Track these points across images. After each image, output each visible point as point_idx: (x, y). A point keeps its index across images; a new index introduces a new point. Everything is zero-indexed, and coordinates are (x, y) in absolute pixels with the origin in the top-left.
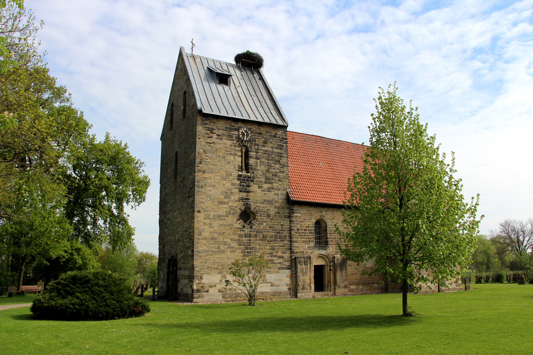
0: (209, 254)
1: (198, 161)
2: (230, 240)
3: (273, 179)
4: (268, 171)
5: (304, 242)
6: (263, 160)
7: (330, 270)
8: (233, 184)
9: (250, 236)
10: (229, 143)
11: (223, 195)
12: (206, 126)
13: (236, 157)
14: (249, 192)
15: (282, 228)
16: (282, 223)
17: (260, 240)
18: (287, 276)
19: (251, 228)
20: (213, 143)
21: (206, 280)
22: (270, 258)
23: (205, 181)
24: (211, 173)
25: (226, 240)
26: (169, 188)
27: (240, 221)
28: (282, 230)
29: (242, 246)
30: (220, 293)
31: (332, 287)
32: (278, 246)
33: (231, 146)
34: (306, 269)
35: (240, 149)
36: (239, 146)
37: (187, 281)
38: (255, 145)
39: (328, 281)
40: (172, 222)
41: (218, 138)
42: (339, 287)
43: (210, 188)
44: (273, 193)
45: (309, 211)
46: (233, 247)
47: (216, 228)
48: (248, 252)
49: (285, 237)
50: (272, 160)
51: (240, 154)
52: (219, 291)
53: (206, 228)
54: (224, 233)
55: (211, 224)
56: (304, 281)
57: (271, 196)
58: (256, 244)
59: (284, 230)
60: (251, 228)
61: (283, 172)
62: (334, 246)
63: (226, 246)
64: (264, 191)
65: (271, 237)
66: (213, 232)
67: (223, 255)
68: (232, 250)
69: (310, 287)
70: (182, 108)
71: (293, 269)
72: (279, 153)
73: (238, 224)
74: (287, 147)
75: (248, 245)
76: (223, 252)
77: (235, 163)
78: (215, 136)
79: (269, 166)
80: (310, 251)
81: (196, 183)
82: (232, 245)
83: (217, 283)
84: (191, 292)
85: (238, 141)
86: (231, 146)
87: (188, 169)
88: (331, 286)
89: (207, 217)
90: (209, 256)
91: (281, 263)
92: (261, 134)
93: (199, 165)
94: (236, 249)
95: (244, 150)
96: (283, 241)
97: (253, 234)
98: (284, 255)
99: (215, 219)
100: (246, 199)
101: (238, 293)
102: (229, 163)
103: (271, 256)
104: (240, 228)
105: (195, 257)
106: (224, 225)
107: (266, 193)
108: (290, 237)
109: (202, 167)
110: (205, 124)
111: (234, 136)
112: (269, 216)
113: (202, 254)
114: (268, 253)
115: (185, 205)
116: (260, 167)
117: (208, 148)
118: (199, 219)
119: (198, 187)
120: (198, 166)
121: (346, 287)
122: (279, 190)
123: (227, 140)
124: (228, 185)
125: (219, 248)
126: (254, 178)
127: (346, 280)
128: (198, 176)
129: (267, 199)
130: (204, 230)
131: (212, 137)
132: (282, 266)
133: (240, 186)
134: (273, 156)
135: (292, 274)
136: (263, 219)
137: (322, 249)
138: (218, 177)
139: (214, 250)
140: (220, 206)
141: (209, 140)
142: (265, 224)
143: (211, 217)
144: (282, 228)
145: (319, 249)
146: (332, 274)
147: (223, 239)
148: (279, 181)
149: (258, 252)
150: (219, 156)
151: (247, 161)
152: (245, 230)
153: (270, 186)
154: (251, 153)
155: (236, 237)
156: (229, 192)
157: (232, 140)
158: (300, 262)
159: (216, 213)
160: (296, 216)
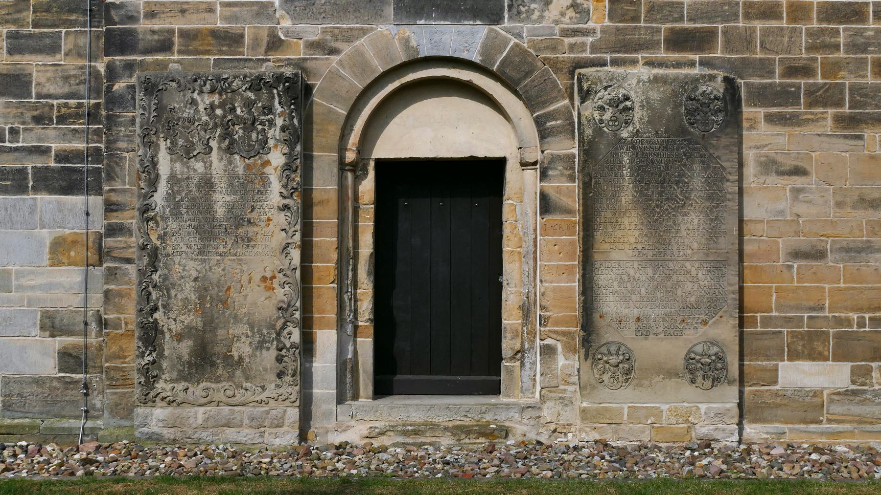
34: (249, 188)
56: (213, 300)
71: (125, 186)
80: (313, 31)
98: (35, 65)
135: (113, 230)
158: (164, 123)
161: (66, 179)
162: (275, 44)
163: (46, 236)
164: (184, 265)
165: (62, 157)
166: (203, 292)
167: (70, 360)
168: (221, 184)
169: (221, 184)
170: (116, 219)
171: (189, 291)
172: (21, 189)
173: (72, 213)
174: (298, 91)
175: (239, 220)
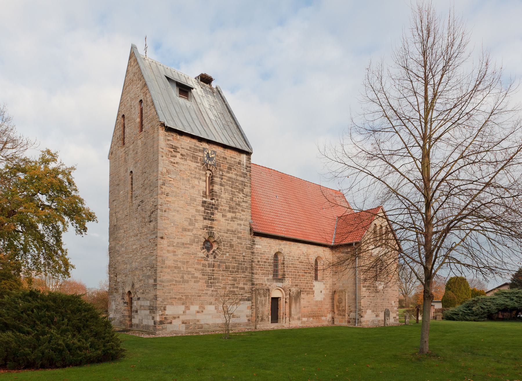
2: (193, 270)
4: (232, 199)
5: (263, 274)
6: (227, 187)
7: (286, 302)
8: (197, 211)
13: (200, 182)
14: (213, 220)
15: (244, 259)
16: (244, 255)
17: (223, 270)
18: (248, 307)
19: (215, 257)
21: (170, 311)
22: (232, 289)
23: (169, 205)
25: (189, 269)
28: (244, 262)
29: (205, 277)
30: (184, 325)
31: (288, 319)
32: (240, 277)
34: (265, 301)
36: (204, 170)
37: (148, 312)
39: (283, 313)
42: (293, 319)
43: (174, 213)
45: (269, 243)
46: (196, 277)
47: (180, 256)
48: (211, 283)
49: (246, 268)
51: (205, 178)
52: (183, 323)
53: (170, 255)
54: (188, 262)
55: (175, 252)
56: (263, 313)
57: (234, 226)
58: (219, 274)
60: (215, 257)
62: (290, 279)
63: (190, 276)
69: (269, 318)
71: (254, 300)
72: (242, 181)
73: (202, 254)
74: (250, 176)
75: (211, 275)
76: (187, 282)
77: (200, 188)
79: (233, 194)
80: (269, 283)
83: (181, 315)
84: (153, 324)
88: (286, 318)
89: (171, 244)
90: (172, 286)
94: (200, 279)
95: (208, 175)
96: (244, 272)
97: (217, 264)
98: (245, 286)
99: (178, 247)
100: (210, 227)
101: (201, 325)
102: (193, 187)
103: (233, 288)
106: (187, 253)
107: (229, 222)
108: (252, 268)
112: (231, 246)
115: (145, 230)
118: (162, 246)
121: (299, 319)
122: (242, 220)
124: (193, 211)
125: (183, 277)
126: (218, 205)
127: (300, 312)
130: (167, 257)
133: (205, 213)
134: (237, 184)
135: (252, 305)
136: (226, 249)
137: (280, 282)
138: (182, 202)
139: (177, 279)
140: (185, 233)
142: (227, 254)
143: (174, 244)
144: (244, 259)
145: (277, 282)
146: (287, 306)
147: (187, 268)
148: (243, 211)
152: (209, 259)
153: (233, 215)
154: (215, 179)
155: (200, 267)
156: (193, 219)
158: (259, 294)
159: (180, 241)
160: (257, 248)
163: (247, 306)
164: (260, 309)
167: (249, 320)
171: (261, 312)
173: (249, 303)
174: (269, 290)
175: (265, 304)
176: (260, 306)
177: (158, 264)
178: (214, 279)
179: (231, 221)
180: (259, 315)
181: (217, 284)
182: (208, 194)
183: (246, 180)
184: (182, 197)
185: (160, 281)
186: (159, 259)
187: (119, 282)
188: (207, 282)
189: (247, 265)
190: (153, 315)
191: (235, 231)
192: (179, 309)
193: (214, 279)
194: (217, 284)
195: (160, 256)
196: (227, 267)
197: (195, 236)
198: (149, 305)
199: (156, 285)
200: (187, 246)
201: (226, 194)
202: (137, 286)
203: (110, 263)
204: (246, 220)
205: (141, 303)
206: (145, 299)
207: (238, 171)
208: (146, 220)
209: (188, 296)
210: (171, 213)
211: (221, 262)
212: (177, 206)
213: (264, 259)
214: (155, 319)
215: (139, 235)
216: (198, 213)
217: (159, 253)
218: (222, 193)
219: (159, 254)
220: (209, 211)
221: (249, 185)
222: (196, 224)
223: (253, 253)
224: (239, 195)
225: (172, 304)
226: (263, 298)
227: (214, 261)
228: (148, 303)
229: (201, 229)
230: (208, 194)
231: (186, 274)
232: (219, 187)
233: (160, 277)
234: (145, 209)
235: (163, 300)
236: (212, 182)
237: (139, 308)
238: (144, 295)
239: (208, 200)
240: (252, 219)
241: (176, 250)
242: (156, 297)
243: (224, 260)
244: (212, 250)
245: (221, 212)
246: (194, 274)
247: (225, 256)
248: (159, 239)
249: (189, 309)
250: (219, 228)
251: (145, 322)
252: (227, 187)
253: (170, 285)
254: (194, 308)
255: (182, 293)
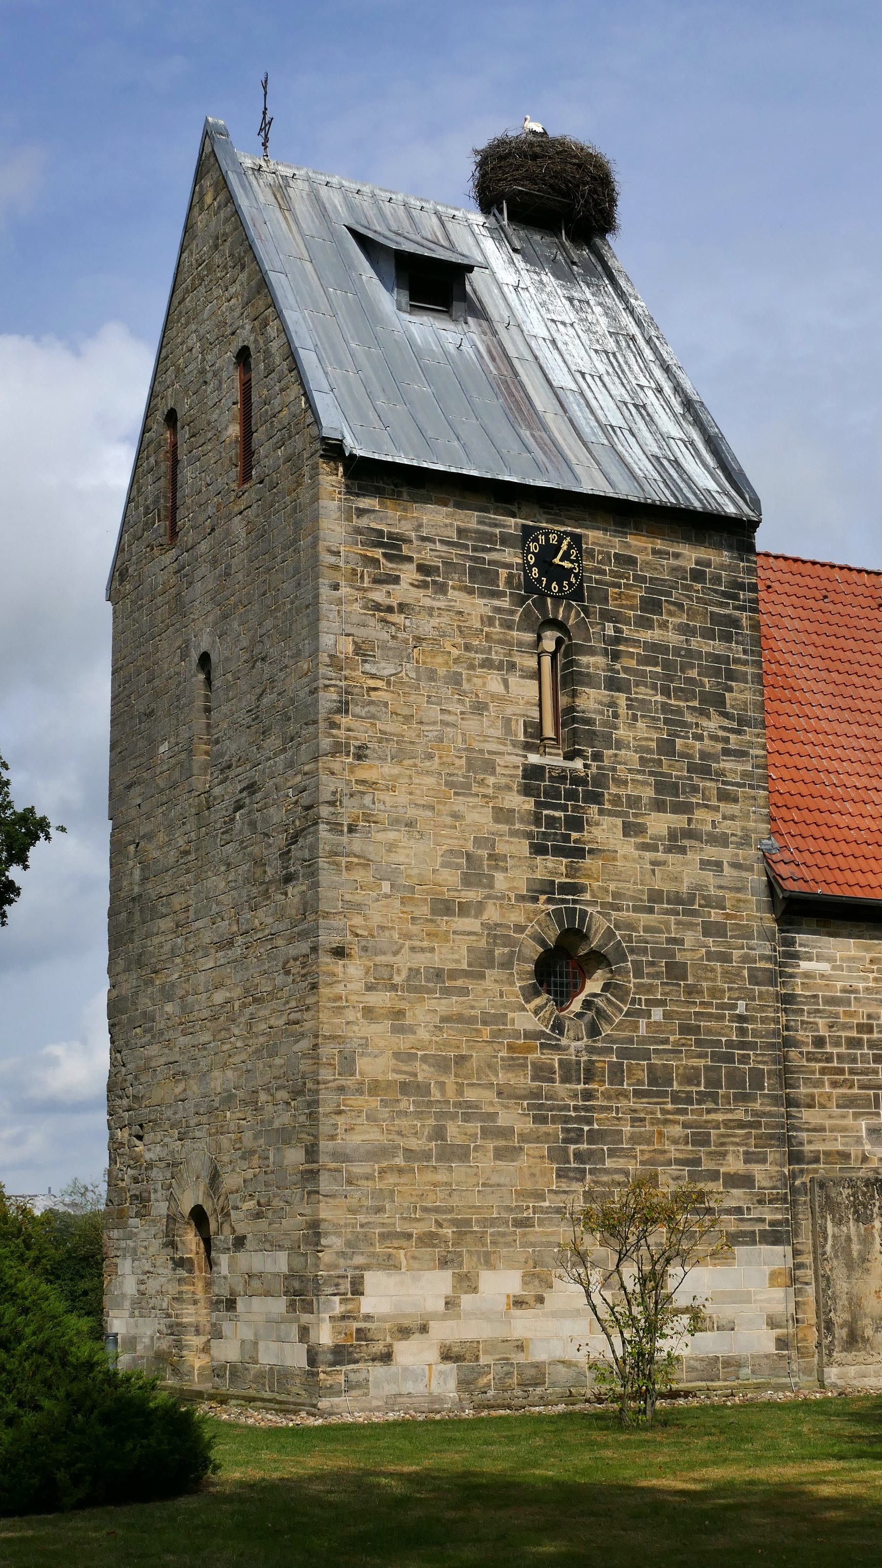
0: (391, 1168)
1: (328, 699)
2: (490, 1095)
3: (695, 789)
4: (667, 747)
5: (848, 1102)
6: (642, 693)
8: (502, 815)
9: (590, 1075)
10: (478, 607)
11: (458, 867)
12: (364, 522)
13: (513, 680)
14: (579, 853)
15: (742, 1032)
16: (741, 1009)
17: (638, 1094)
18: (773, 1276)
19: (594, 1031)
20: (402, 608)
24: (398, 758)
25: (471, 1095)
26: (162, 837)
27: (538, 1001)
28: (743, 1045)
29: (550, 1128)
30: (450, 1366)
32: (727, 1124)
33: (490, 621)
35: (529, 637)
37: (279, 1305)
38: (607, 616)
40: (185, 1009)
41: (424, 585)
43: (392, 835)
44: (693, 857)
45: (868, 949)
46: (506, 1133)
47: (423, 1034)
48: (578, 1156)
49: (757, 1077)
50: (685, 694)
51: (532, 663)
52: (447, 1356)
53: (378, 1032)
54: (461, 1059)
55: (399, 1014)
56: (855, 1303)
57: (686, 871)
58: (619, 1111)
59: (753, 1046)
60: (594, 1031)
61: (741, 754)
63: (475, 1127)
64: (655, 848)
65: (691, 1078)
66: (412, 1057)
67: (459, 1171)
68: (502, 1143)
70: (234, 430)
71: (805, 1240)
72: (717, 658)
73: (527, 1019)
74: (756, 626)
75: (579, 1120)
76: (462, 1154)
77: (509, 710)
78: (408, 573)
79: (674, 722)
81: (325, 811)
82: (503, 1121)
83: (434, 1316)
84: (302, 1362)
85: (522, 600)
86: (490, 621)
87: (273, 742)
90: (392, 1179)
91: (739, 1210)
92: (632, 561)
93: (337, 718)
94: (523, 1138)
95: (549, 645)
96: (744, 1098)
98: (756, 1169)
100: (565, 888)
101: (537, 1366)
102: (479, 708)
104: (542, 1034)
105: (325, 1184)
106: (459, 1018)
107: (660, 855)
108: (786, 1076)
109: (354, 727)
110: (361, 512)
111: (503, 573)
112: (676, 971)
113: (358, 1169)
114: (678, 1162)
116: (632, 727)
117: (375, 632)
118: (339, 989)
119: (335, 827)
120: (334, 725)
122: (722, 840)
123: (470, 592)
124: (480, 818)
125: (439, 1133)
126: (600, 780)
128: (335, 777)
129: (666, 887)
130: (365, 1043)
131: (396, 580)
132: (746, 1227)
133: (537, 821)
134: (693, 673)
135: (798, 1266)
136: (650, 989)
138: (430, 781)
139: (414, 1143)
141: (378, 596)
142: (657, 1014)
143: (397, 979)
144: (742, 1032)
148: (724, 796)
149: (629, 1155)
150: (432, 675)
151: (563, 701)
152: (564, 1042)
153: (679, 821)
154: (584, 659)
155: (524, 1081)
156: (485, 853)
157: (499, 595)
158: (830, 1205)
159: (421, 960)
160: (807, 975)
161: (774, 1237)
162: (865, 1159)
163: (767, 1269)
164: (841, 1286)
165: (772, 1223)
166: (850, 1300)
167: (782, 1343)
168: (855, 1239)
169: (855, 1239)
170: (799, 1259)
171: (843, 1301)
172: (754, 1243)
173: (777, 1256)
175: (864, 1260)
176: (837, 1270)
177: (325, 1074)
178: (593, 1137)
179: (669, 850)
180: (839, 1317)
181: (609, 1163)
182: (549, 731)
183: (736, 650)
184: (430, 757)
185: (336, 1155)
186: (327, 1050)
187: (150, 1166)
188: (558, 1155)
189: (759, 1061)
190: (306, 1318)
191: (691, 899)
192: (429, 1288)
193: (593, 1137)
194: (609, 1163)
195: (333, 1037)
196: (659, 1078)
197: (495, 933)
198: (285, 1269)
199: (312, 1175)
200: (459, 983)
201: (640, 724)
202: (230, 1181)
203: (112, 1075)
204: (745, 841)
205: (253, 1260)
206: (271, 1244)
207: (692, 614)
208: (270, 871)
209: (468, 1222)
210: (380, 837)
211: (623, 1053)
212: (403, 799)
213: (846, 1027)
214: (312, 1339)
215: (240, 940)
216: (504, 828)
217: (328, 1022)
218: (620, 722)
219: (326, 1030)
220: (557, 814)
221: (750, 670)
222: (499, 876)
223: (788, 999)
224: (705, 723)
225: (389, 1264)
226: (852, 1228)
227: (591, 1050)
228: (280, 1262)
229: (521, 898)
230: (549, 731)
231: (453, 1117)
232: (603, 694)
233: (333, 1137)
234: (265, 820)
235: (349, 1244)
236: (568, 678)
237: (240, 1289)
238: (263, 1224)
239: (554, 760)
240: (772, 833)
241: (404, 1005)
242: (314, 1231)
243: (643, 1040)
244: (582, 997)
245: (617, 814)
246: (493, 1116)
247: (643, 1022)
248: (326, 959)
249: (475, 1290)
250: (612, 887)
251: (268, 1355)
252: (642, 693)
253: (382, 1171)
254: (500, 1283)
255: (437, 1210)
